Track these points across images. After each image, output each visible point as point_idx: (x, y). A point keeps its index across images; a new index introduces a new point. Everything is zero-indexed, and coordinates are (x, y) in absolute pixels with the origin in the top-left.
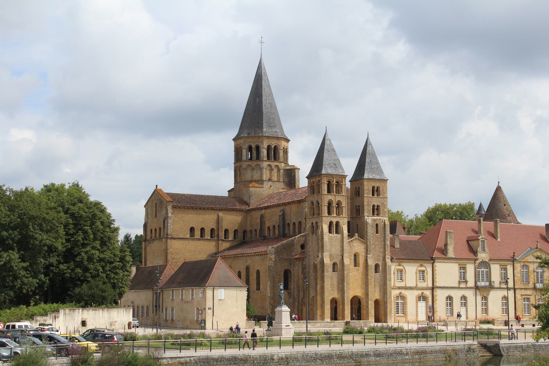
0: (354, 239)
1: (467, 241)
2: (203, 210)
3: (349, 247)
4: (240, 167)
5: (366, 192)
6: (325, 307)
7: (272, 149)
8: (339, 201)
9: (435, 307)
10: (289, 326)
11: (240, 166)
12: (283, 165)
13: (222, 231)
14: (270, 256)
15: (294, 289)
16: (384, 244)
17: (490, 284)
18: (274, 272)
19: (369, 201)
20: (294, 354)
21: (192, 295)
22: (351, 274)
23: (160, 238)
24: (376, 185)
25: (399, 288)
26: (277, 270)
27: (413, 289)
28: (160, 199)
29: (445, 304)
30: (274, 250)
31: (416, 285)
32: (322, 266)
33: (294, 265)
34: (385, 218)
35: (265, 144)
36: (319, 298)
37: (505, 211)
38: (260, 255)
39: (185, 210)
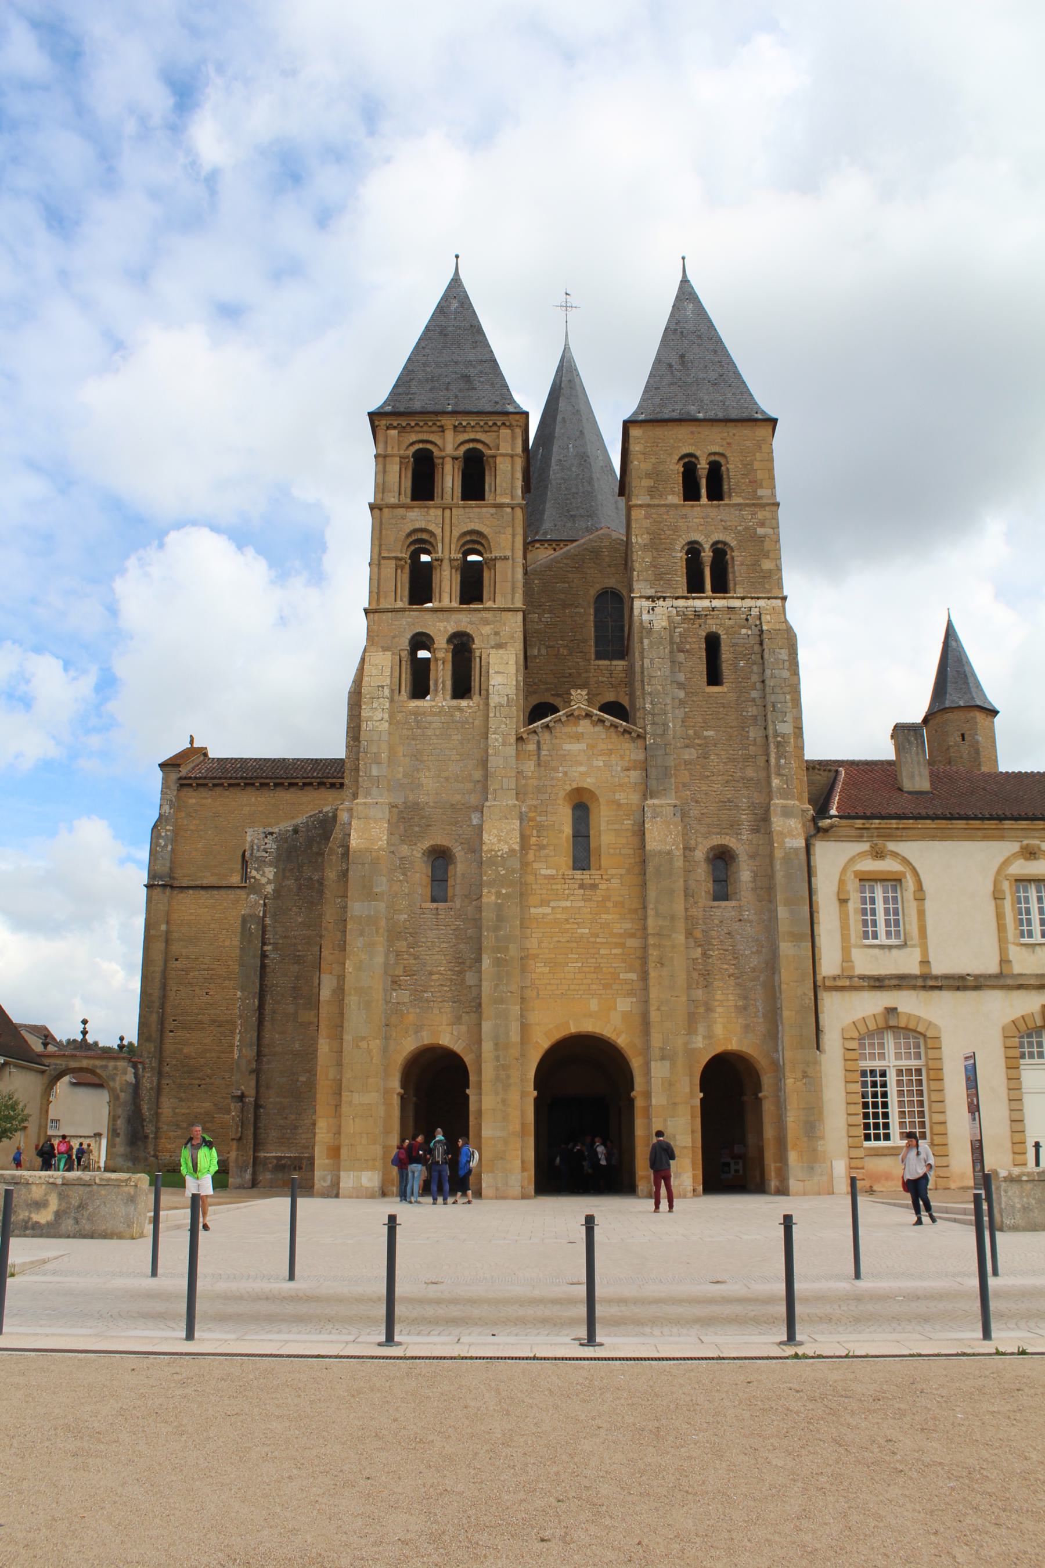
2: (292, 790)
6: (344, 1098)
8: (474, 541)
16: (759, 741)
22: (548, 910)
25: (878, 983)
26: (285, 937)
27: (977, 988)
30: (271, 844)
31: (1004, 961)
34: (761, 603)
39: (227, 793)
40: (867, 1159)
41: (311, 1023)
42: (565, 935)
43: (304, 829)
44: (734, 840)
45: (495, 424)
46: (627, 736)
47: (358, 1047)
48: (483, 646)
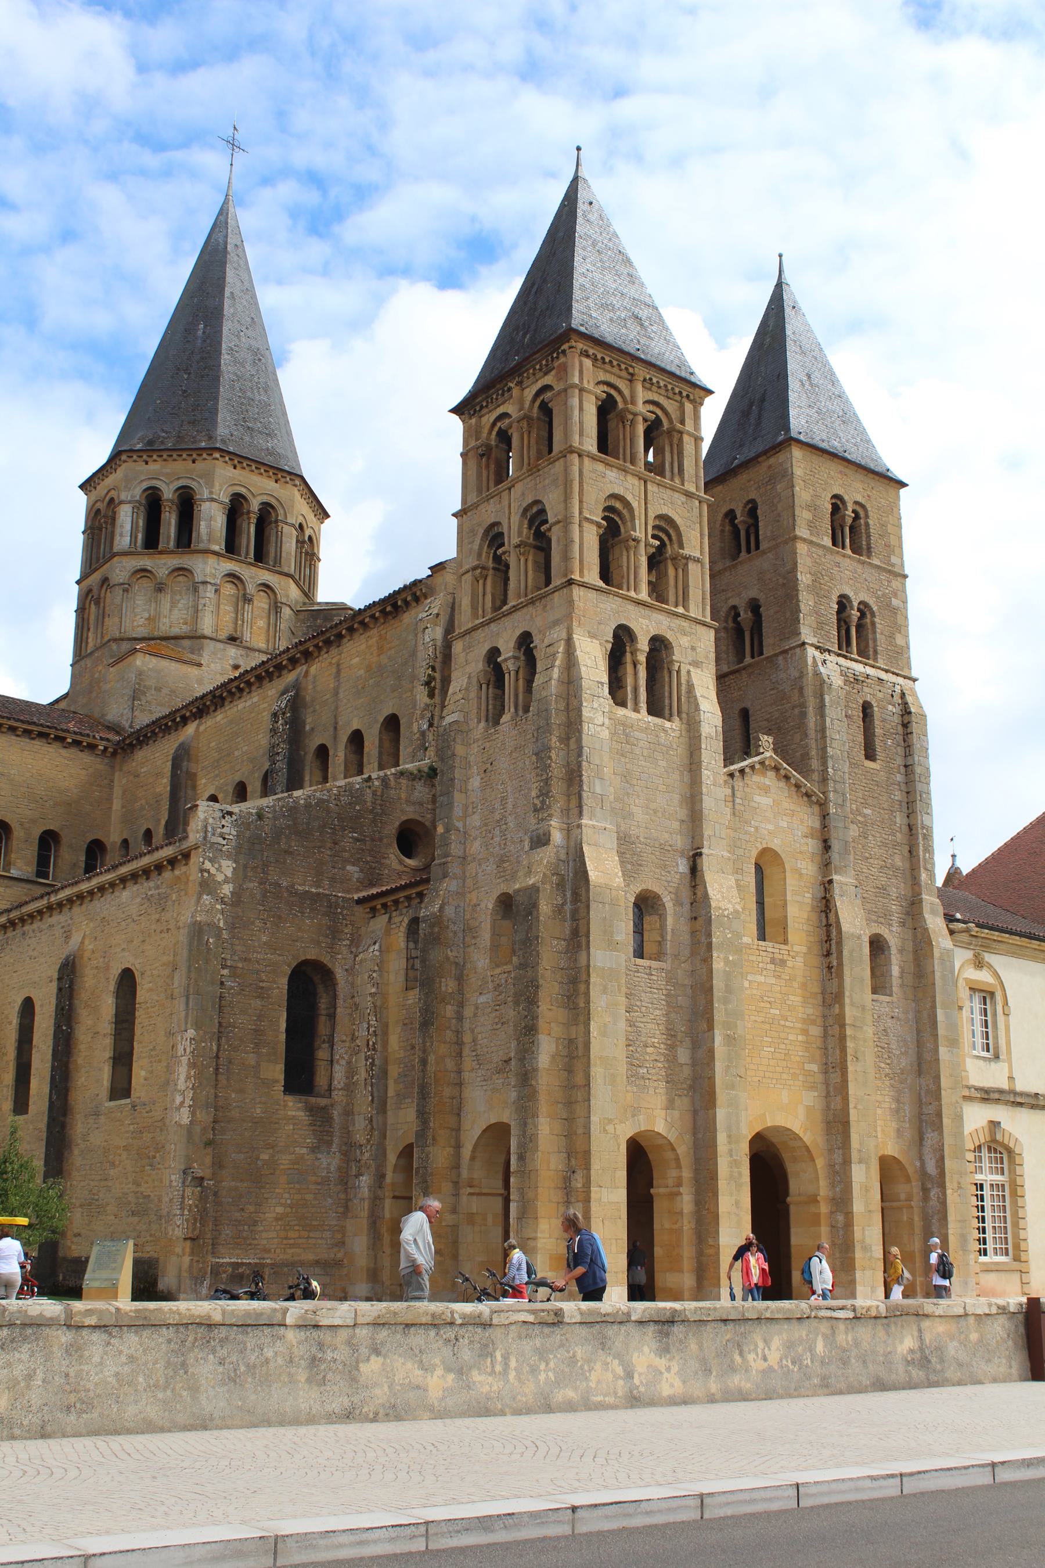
0: (752, 767)
3: (728, 811)
4: (102, 586)
5: (803, 516)
6: (593, 1196)
7: (249, 512)
11: (105, 580)
12: (292, 592)
14: (207, 865)
15: (350, 1088)
16: (905, 829)
18: (225, 972)
24: (854, 491)
25: (988, 1096)
26: (246, 960)
30: (231, 831)
32: (568, 907)
33: (355, 941)
34: (900, 680)
35: (221, 485)
38: (146, 872)
40: (981, 1275)
41: (277, 1081)
42: (761, 1014)
43: (270, 816)
44: (887, 931)
45: (680, 393)
46: (805, 799)
47: (605, 1130)
48: (682, 660)
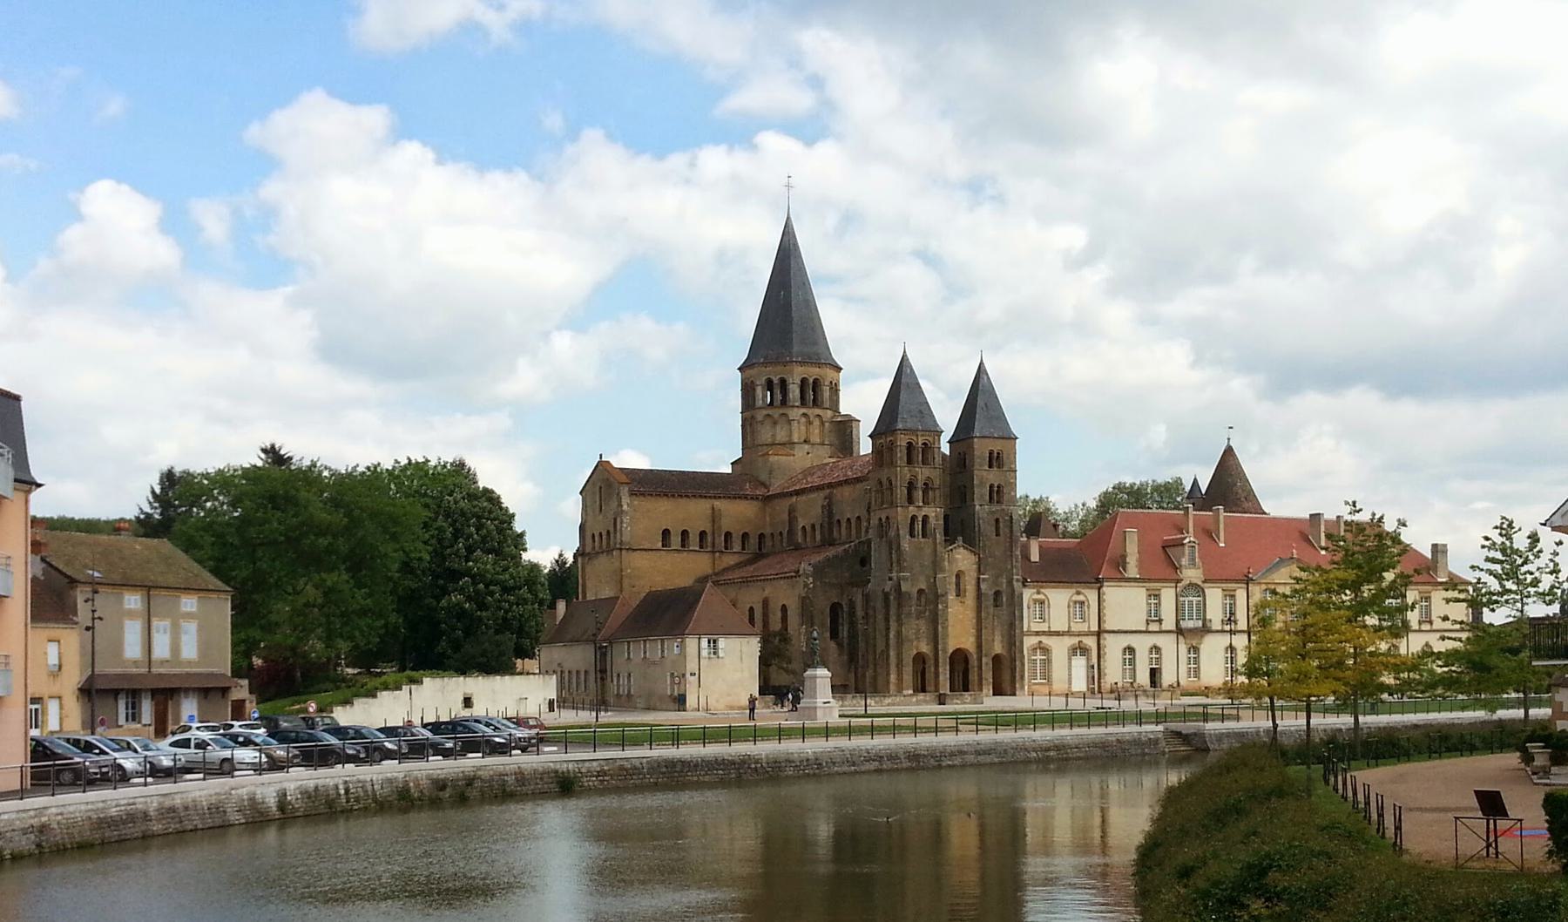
1: (1163, 547)
2: (685, 498)
5: (977, 461)
9: (1102, 667)
10: (829, 702)
11: (753, 417)
13: (720, 536)
17: (1204, 624)
19: (984, 476)
20: (829, 752)
21: (663, 651)
23: (609, 551)
24: (997, 446)
25: (1037, 633)
27: (1062, 635)
28: (608, 479)
29: (1121, 661)
31: (1069, 627)
36: (892, 653)
37: (1240, 491)
38: (788, 578)
